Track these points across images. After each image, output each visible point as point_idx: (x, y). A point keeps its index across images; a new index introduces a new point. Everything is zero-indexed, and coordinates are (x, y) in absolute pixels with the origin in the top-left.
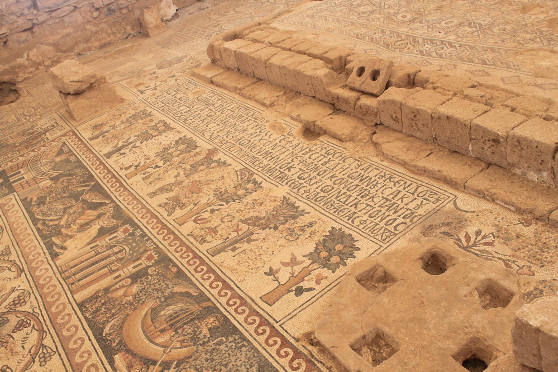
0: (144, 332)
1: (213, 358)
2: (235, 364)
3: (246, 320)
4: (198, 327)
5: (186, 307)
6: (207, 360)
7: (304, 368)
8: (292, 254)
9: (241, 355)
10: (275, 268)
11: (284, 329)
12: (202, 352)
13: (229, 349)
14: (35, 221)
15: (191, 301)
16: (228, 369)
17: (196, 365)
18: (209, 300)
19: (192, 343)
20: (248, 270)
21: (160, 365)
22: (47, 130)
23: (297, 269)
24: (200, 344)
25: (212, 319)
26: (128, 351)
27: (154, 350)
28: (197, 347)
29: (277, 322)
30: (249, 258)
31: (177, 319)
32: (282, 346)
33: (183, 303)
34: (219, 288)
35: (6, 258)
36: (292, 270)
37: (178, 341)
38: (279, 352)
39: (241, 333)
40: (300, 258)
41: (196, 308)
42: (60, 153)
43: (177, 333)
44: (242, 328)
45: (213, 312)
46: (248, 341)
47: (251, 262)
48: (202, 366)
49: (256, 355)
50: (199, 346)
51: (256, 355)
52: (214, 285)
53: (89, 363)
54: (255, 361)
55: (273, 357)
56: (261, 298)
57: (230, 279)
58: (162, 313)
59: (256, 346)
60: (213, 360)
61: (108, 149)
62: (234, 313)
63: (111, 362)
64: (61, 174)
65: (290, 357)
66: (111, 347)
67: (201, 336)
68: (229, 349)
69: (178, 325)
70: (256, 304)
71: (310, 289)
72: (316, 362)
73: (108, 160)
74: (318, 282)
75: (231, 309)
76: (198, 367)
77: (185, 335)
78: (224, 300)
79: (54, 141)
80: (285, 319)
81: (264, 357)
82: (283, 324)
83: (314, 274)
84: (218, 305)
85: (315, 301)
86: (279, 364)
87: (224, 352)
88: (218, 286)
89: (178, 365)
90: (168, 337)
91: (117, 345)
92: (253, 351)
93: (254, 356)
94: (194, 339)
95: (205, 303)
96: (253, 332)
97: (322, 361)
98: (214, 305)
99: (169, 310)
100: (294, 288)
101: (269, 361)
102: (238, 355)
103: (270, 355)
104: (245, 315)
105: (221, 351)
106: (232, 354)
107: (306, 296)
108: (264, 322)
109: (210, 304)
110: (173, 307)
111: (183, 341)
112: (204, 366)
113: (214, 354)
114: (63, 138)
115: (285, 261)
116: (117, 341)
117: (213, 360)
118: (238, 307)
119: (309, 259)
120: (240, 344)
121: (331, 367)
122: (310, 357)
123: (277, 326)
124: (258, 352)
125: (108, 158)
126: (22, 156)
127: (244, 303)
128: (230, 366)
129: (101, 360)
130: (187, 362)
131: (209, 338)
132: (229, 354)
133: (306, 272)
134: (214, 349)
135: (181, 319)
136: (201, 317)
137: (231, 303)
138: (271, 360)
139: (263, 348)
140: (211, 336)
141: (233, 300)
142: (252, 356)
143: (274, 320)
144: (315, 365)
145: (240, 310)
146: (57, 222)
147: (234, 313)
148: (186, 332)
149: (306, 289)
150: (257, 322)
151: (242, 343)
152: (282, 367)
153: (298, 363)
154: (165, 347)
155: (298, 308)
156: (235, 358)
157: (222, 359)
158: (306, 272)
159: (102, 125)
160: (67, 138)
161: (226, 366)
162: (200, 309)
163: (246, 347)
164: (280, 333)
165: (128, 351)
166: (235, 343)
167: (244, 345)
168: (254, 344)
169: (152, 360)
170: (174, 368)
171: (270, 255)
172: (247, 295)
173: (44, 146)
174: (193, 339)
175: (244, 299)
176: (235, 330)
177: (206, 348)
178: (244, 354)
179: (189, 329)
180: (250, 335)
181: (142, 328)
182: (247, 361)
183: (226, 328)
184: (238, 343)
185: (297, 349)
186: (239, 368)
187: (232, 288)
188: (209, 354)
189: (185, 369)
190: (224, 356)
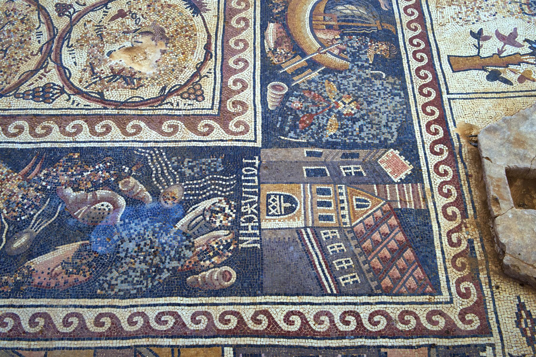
0: (311, 17)
1: (361, 88)
2: (379, 107)
3: (418, 70)
4: (366, 46)
5: (367, 17)
6: (354, 85)
7: (444, 158)
8: (515, 29)
9: (391, 102)
10: (485, 33)
11: (450, 105)
12: (355, 74)
13: (382, 89)
15: (375, 13)
16: (369, 108)
17: (341, 84)
18: (395, 24)
19: (350, 59)
20: (455, 16)
21: (307, 61)
23: (510, 50)
24: (358, 65)
25: (384, 47)
26: (285, 26)
27: (309, 41)
28: (353, 67)
29: (448, 93)
30: (465, 3)
31: (350, 24)
32: (436, 121)
33: (366, 10)
34: (413, 18)
36: (503, 47)
37: (338, 48)
38: (430, 126)
39: (404, 81)
40: (520, 39)
41: (375, 25)
43: (342, 39)
44: (409, 76)
45: (391, 41)
46: (406, 94)
47: (464, 9)
48: (346, 89)
49: (405, 112)
50: (355, 66)
51: (405, 112)
52: (409, 11)
53: (243, 15)
54: (400, 117)
55: (420, 126)
56: (449, 56)
57: (430, 16)
58: (340, 8)
59: (411, 103)
60: (360, 89)
62: (410, 55)
63: (264, 27)
65: (437, 137)
66: (271, 11)
67: (364, 57)
68: (382, 89)
69: (348, 31)
70: (440, 60)
71: (506, 81)
72: (459, 160)
74: (522, 79)
75: (411, 49)
76: (342, 87)
77: (348, 46)
78: (409, 34)
80: (458, 96)
81: (412, 120)
82: (453, 99)
83: (523, 68)
84: (400, 36)
85: (503, 98)
86: (422, 136)
87: (376, 89)
88: (413, 14)
89: (324, 72)
90: (331, 37)
91: (277, 14)
92: (405, 106)
93: (402, 113)
94: (355, 57)
95: (388, 25)
96: (418, 87)
97: (467, 163)
98: (397, 32)
99: (348, 9)
100: (490, 69)
101: (413, 128)
102: (388, 101)
103: (419, 122)
104: (420, 64)
105: (374, 85)
106: (382, 96)
107: (497, 86)
108: (435, 84)
109: (392, 29)
110: (354, 8)
111: (342, 51)
112: (348, 89)
113: (366, 84)
115: (502, 32)
116: (280, 10)
117: (360, 89)
118: (419, 51)
119: (530, 47)
120: (396, 91)
121: (471, 176)
122: (457, 151)
123: (445, 97)
124: (409, 111)
127: (428, 51)
128: (373, 106)
129: (255, 19)
130: (334, 75)
131: (370, 64)
132: (379, 94)
133: (517, 59)
134: (368, 79)
135: (354, 26)
136: (374, 38)
137: (415, 42)
138: (416, 128)
139: (417, 110)
140: (372, 64)
141: (418, 40)
142: (400, 111)
143: (447, 89)
144: (457, 163)
145: (418, 55)
147: (410, 55)
148: (351, 44)
149: (502, 78)
150: (428, 80)
151: (399, 92)
152: (423, 141)
153: (440, 149)
154: (323, 46)
155: (480, 93)
156: (383, 102)
157: (370, 95)
158: (517, 59)
161: (369, 103)
162: (380, 28)
163: (400, 98)
164: (443, 106)
165: (285, 26)
166: (392, 87)
167: (399, 95)
168: (410, 101)
169: (302, 50)
170: (319, 73)
171: (491, 15)
172: (437, 45)
174: (353, 55)
175: (430, 46)
176: (401, 74)
177: (361, 73)
178: (393, 104)
179: (356, 43)
180: (413, 88)
181: (312, 11)
182: (392, 112)
183: (392, 65)
184: (396, 89)
185: (450, 135)
186: (380, 115)
187: (426, 26)
188: (360, 81)
189: (329, 80)
190: (374, 93)
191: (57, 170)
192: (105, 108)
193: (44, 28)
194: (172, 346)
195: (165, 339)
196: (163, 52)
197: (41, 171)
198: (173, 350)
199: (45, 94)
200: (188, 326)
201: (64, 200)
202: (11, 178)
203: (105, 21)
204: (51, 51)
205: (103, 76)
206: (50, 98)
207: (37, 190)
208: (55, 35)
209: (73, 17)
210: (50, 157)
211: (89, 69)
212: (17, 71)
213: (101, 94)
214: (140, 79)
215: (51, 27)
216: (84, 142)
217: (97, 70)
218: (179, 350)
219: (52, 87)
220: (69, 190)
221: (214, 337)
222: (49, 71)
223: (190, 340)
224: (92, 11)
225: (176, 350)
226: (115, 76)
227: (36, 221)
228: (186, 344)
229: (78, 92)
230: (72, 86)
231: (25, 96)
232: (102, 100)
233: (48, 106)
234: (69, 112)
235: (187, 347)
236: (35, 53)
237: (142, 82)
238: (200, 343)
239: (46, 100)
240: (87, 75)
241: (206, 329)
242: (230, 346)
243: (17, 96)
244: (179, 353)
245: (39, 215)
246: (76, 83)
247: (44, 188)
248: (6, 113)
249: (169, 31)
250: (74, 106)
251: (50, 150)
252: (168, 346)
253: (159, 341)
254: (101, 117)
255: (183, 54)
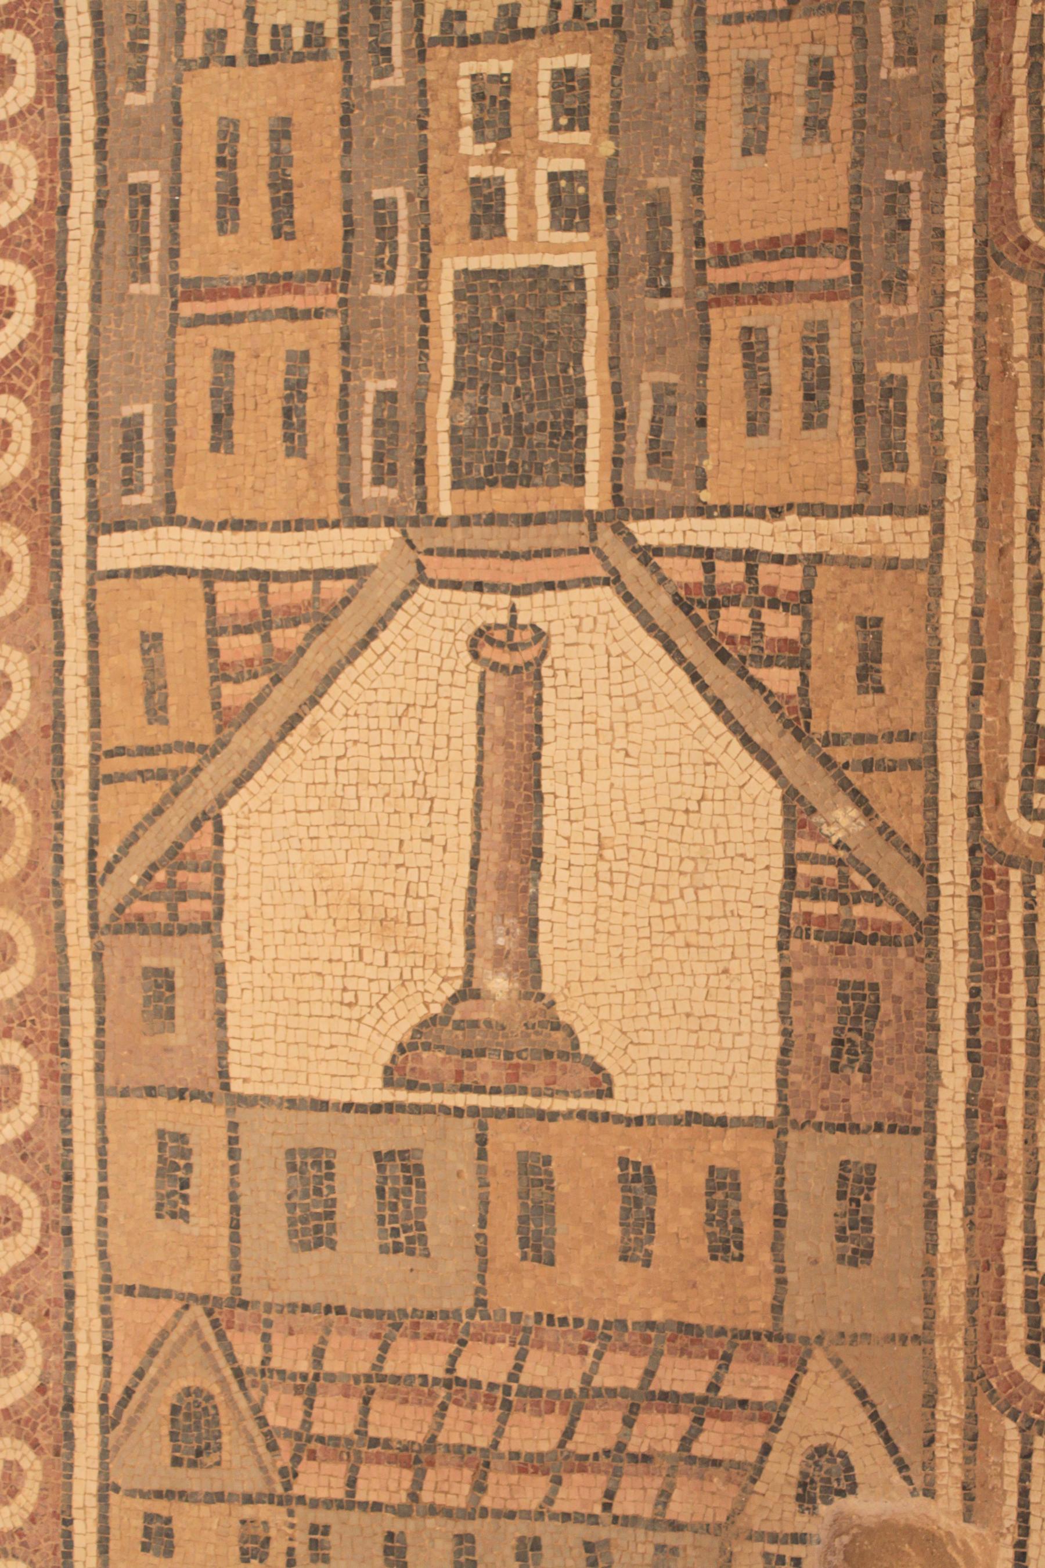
194: (94, 785)
195: (68, 812)
198: (109, 779)
200: (16, 723)
218: (110, 754)
221: (58, 614)
223: (69, 710)
225: (108, 766)
228: (85, 725)
235: (96, 722)
238: (83, 668)
241: (29, 648)
242: (92, 540)
244: (120, 751)
252: (94, 797)
253: (76, 840)
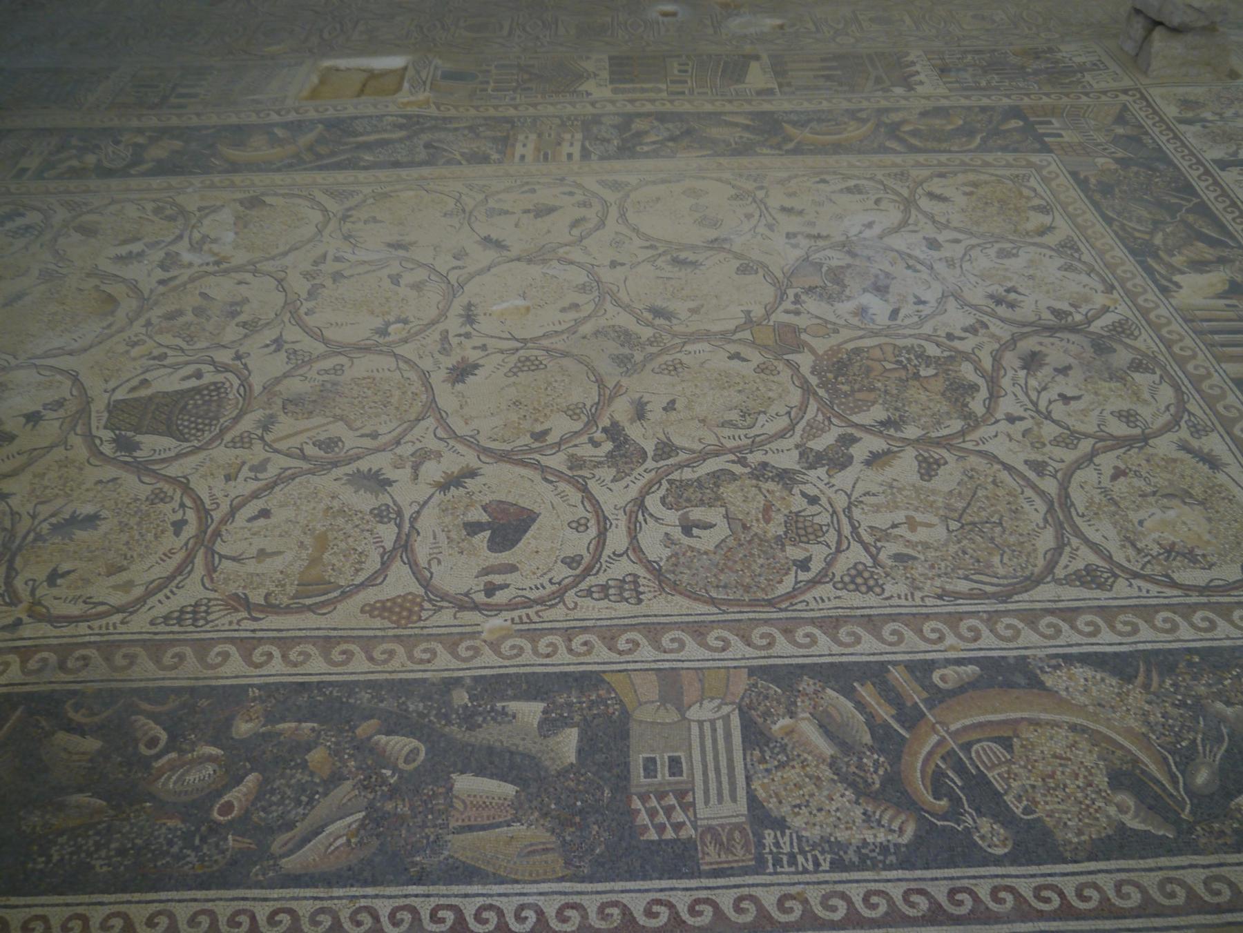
14: (1109, 221)
22: (1082, 69)
35: (1076, 255)
42: (1121, 119)
61: (1218, 153)
64: (1130, 159)
73: (1222, 174)
79: (1105, 93)
114: (1123, 98)
125: (1223, 169)
126: (1047, 95)
146: (1147, 237)
159: (1197, 103)
160: (1131, 99)
173: (1087, 94)
191: (1184, 680)
192: (1187, 595)
193: (1029, 492)
196: (1209, 520)
197: (1164, 682)
199: (1088, 577)
201: (1222, 719)
202: (1129, 691)
203: (1106, 483)
204: (1061, 524)
205: (1155, 554)
206: (1104, 584)
207: (1173, 705)
208: (1052, 503)
209: (1059, 475)
210: (1164, 662)
211: (1128, 544)
212: (1035, 550)
213: (1167, 576)
214: (1204, 556)
215: (1042, 494)
216: (1194, 640)
217: (1139, 545)
219: (1096, 570)
220: (1219, 706)
222: (1077, 549)
224: (1079, 468)
226: (1169, 552)
227: (1204, 747)
229: (1136, 575)
230: (1121, 567)
231: (1068, 581)
232: (1174, 585)
233: (1108, 595)
234: (1143, 601)
236: (1042, 525)
237: (1208, 559)
239: (1100, 586)
240: (1131, 552)
243: (1058, 582)
245: (1203, 740)
246: (1126, 564)
247: (1183, 704)
248: (1060, 605)
249: (1197, 491)
250: (1144, 593)
251: (1157, 652)
254: (1194, 608)
255: (1236, 521)
